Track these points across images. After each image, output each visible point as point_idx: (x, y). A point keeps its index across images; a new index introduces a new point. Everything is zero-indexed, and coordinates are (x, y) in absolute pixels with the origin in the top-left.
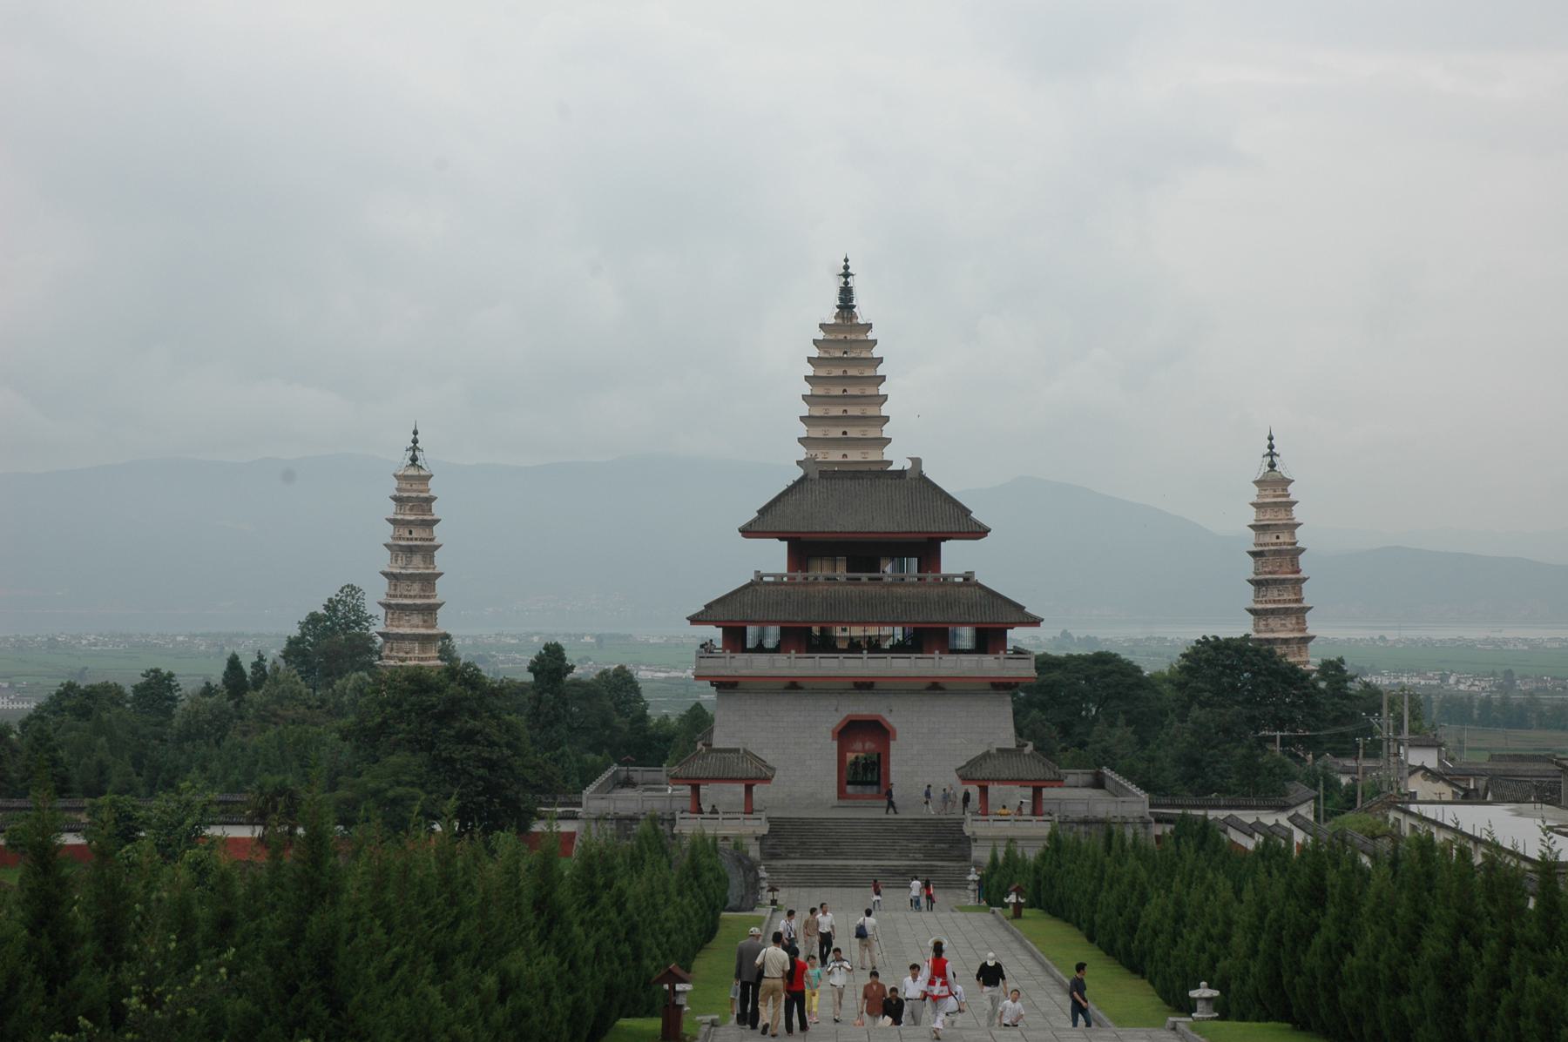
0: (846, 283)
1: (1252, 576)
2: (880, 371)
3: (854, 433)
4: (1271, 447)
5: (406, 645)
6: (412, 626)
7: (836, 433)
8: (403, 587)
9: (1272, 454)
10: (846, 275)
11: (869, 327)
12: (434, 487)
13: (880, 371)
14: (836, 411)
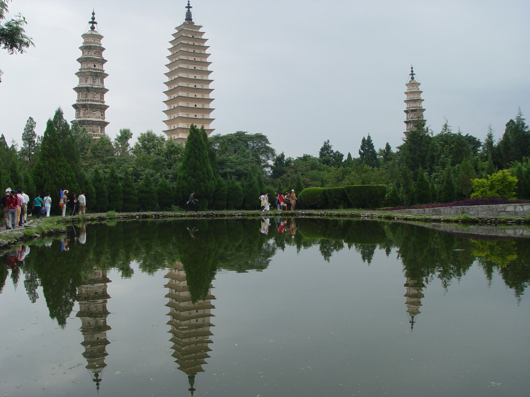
0: (189, 10)
1: (406, 120)
2: (206, 44)
3: (198, 68)
4: (412, 71)
5: (95, 128)
6: (97, 117)
7: (192, 67)
8: (90, 96)
9: (412, 74)
10: (189, 7)
11: (201, 27)
12: (104, 43)
13: (206, 44)
14: (192, 59)
